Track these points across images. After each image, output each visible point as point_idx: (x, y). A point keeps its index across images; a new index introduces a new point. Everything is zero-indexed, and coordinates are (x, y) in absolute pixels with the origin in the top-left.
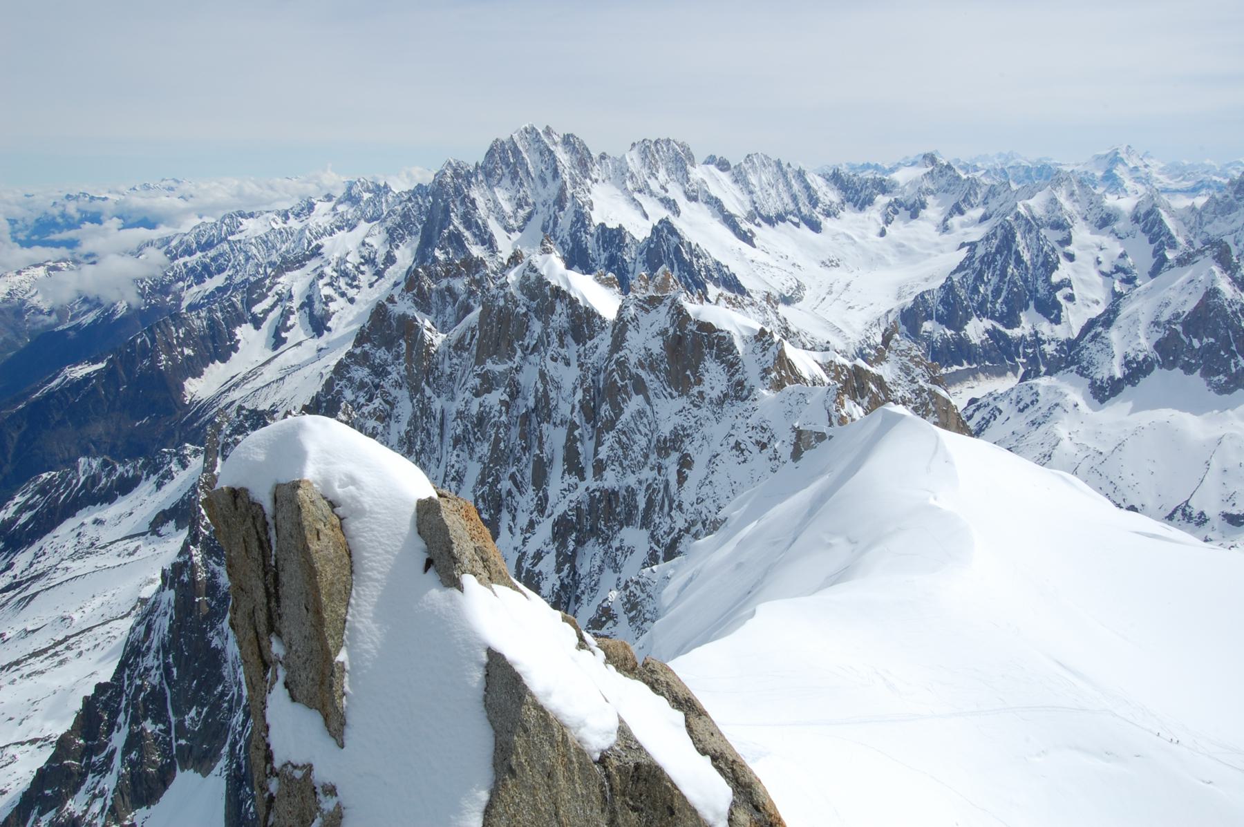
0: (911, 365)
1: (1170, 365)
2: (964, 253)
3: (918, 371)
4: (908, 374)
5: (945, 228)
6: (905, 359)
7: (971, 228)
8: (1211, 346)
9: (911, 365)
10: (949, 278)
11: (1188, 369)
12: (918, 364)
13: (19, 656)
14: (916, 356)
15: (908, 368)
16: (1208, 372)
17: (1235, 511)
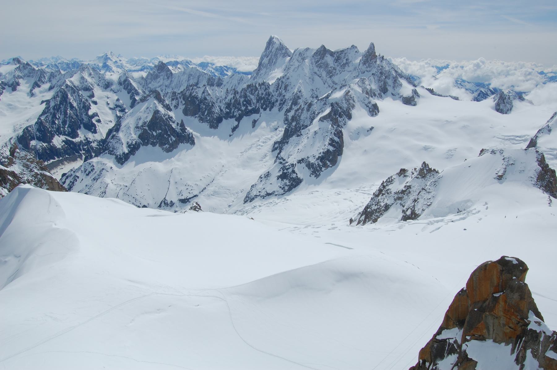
0: (28, 163)
1: (146, 144)
2: (44, 106)
3: (33, 165)
4: (28, 168)
5: (32, 95)
6: (25, 161)
7: (45, 93)
8: (160, 134)
9: (28, 163)
10: (39, 119)
11: (154, 144)
12: (32, 162)
14: (30, 159)
15: (27, 165)
16: (161, 145)
17: (183, 198)
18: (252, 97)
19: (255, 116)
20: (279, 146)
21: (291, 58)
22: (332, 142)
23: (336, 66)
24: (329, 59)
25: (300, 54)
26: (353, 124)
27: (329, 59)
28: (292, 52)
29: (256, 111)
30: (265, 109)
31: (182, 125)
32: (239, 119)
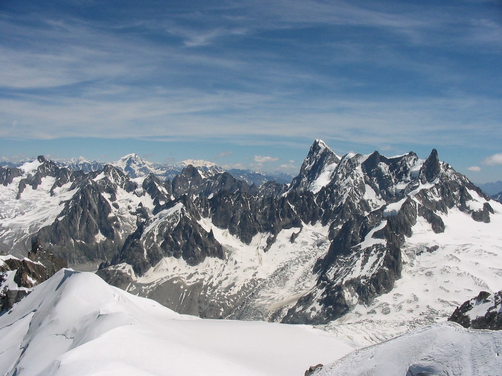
2: (63, 206)
5: (52, 193)
7: (66, 193)
10: (56, 220)
13: (9, 325)
18: (292, 207)
19: (296, 230)
20: (322, 266)
21: (339, 165)
22: (387, 262)
23: (391, 175)
24: (384, 167)
25: (349, 161)
26: (411, 242)
27: (384, 167)
28: (340, 158)
29: (296, 224)
30: (307, 223)
31: (211, 235)
32: (275, 232)
